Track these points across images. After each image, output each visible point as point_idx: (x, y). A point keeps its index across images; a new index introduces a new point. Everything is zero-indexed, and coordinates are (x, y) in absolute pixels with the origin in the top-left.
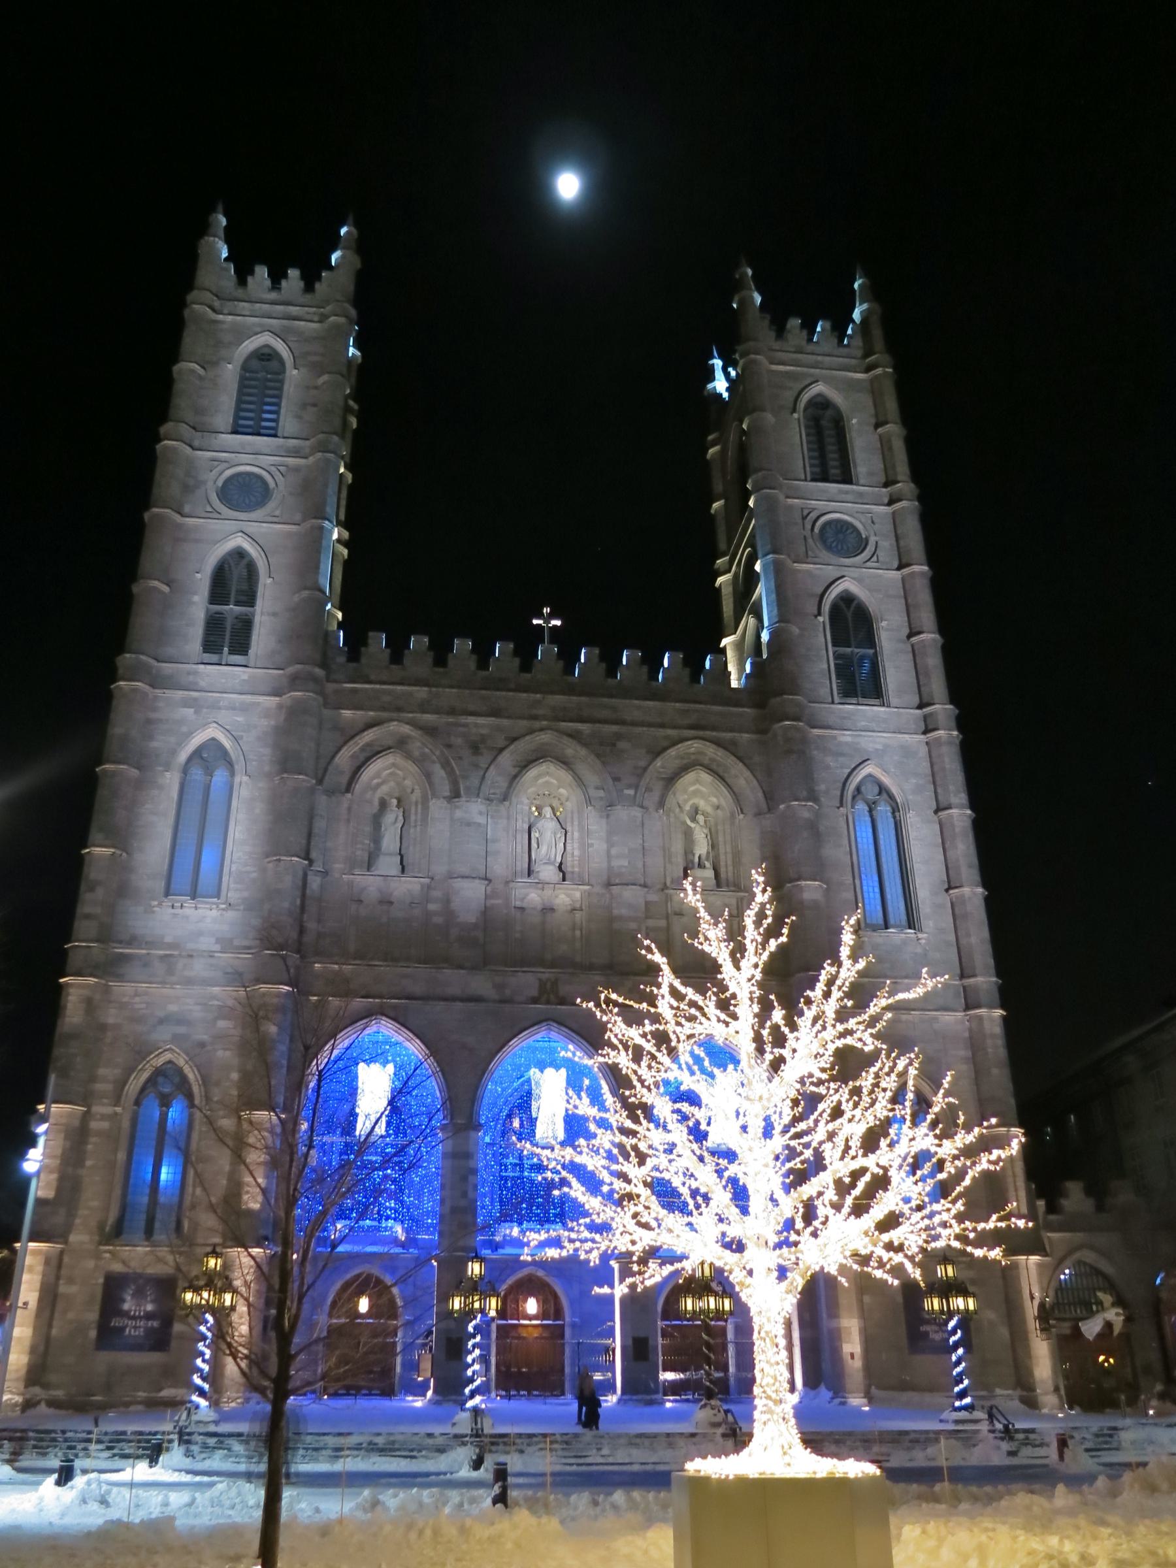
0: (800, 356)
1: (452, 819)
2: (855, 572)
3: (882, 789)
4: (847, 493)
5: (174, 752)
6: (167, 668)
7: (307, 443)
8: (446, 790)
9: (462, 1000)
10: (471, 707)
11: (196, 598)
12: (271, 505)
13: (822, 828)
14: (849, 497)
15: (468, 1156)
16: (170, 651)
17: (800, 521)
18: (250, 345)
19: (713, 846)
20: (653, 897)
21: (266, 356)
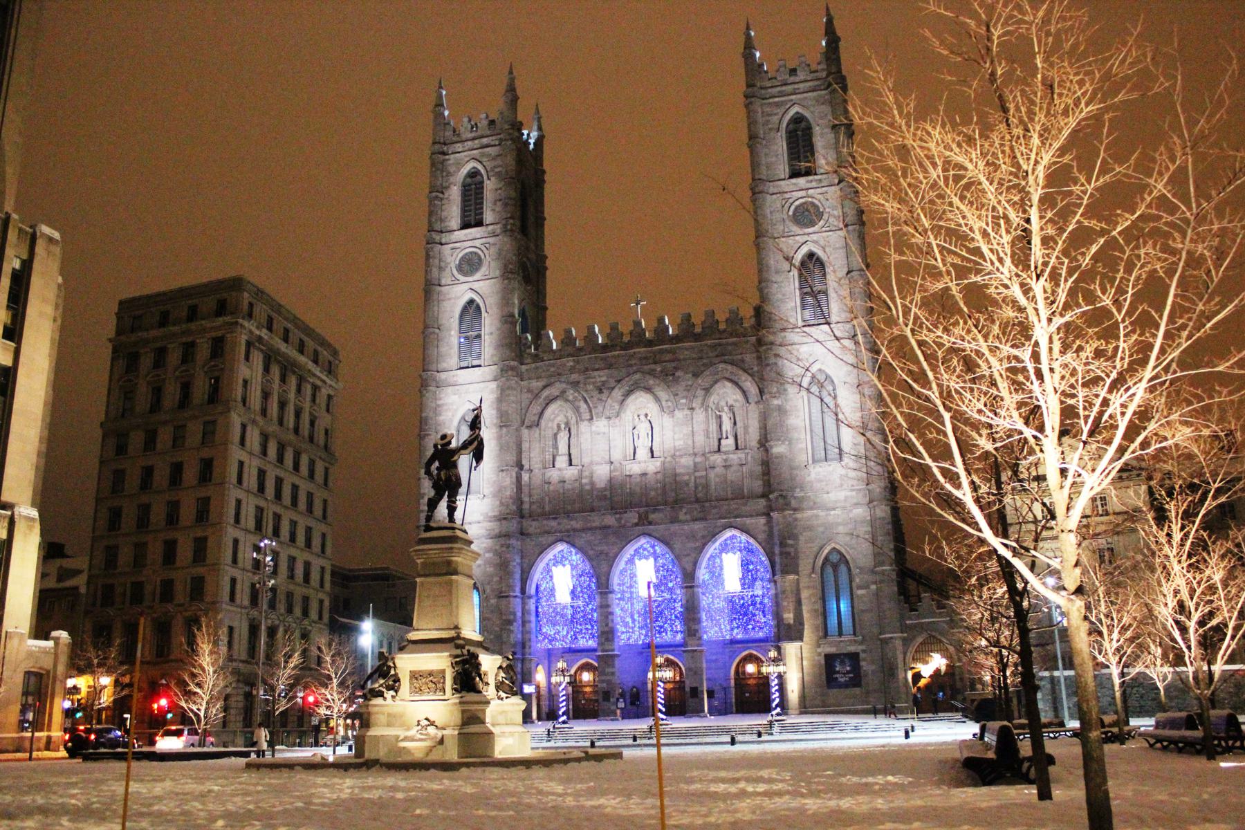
0: (784, 88)
1: (591, 432)
2: (815, 237)
3: (827, 377)
4: (811, 181)
5: (451, 420)
6: (443, 376)
7: (499, 226)
8: (587, 416)
9: (600, 528)
10: (597, 366)
11: (453, 333)
12: (484, 270)
13: (788, 407)
14: (814, 184)
15: (608, 606)
16: (444, 365)
17: (780, 209)
18: (465, 170)
19: (735, 423)
20: (698, 459)
21: (474, 174)
